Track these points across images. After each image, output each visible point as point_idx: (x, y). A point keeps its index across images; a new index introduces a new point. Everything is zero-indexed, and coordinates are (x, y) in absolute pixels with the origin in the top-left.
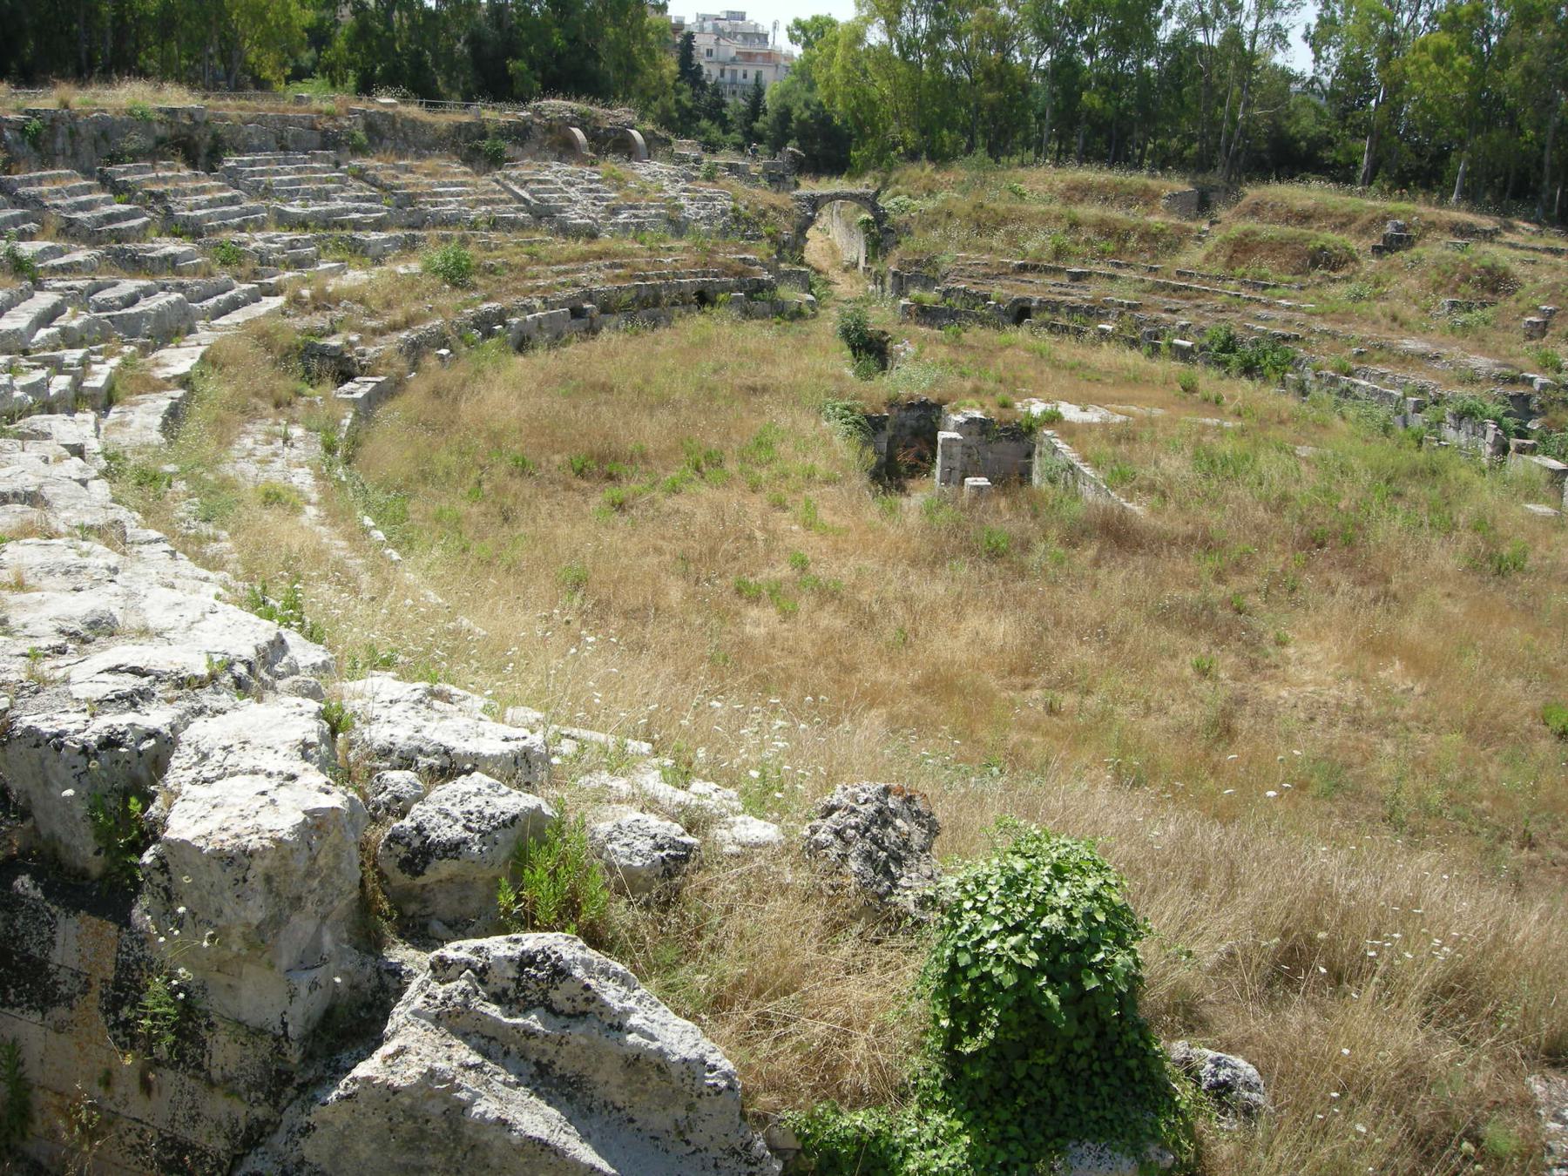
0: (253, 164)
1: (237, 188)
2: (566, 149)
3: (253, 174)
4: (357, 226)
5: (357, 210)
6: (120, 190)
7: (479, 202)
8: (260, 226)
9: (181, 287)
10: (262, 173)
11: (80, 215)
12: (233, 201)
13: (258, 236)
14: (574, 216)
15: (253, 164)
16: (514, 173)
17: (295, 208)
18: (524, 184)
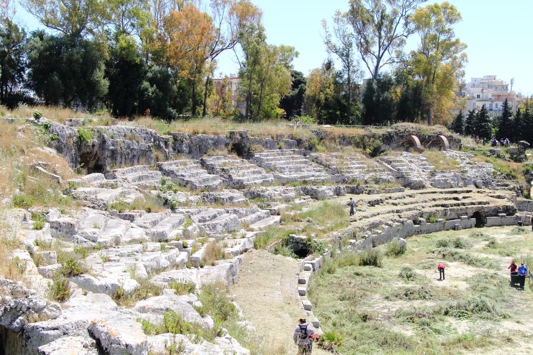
0: (267, 156)
1: (260, 166)
2: (409, 145)
3: (268, 160)
4: (314, 183)
5: (313, 176)
6: (211, 169)
7: (368, 172)
8: (270, 184)
9: (235, 212)
10: (272, 160)
11: (192, 179)
12: (260, 173)
13: (269, 188)
14: (414, 177)
15: (267, 156)
16: (386, 157)
17: (286, 175)
18: (390, 163)
